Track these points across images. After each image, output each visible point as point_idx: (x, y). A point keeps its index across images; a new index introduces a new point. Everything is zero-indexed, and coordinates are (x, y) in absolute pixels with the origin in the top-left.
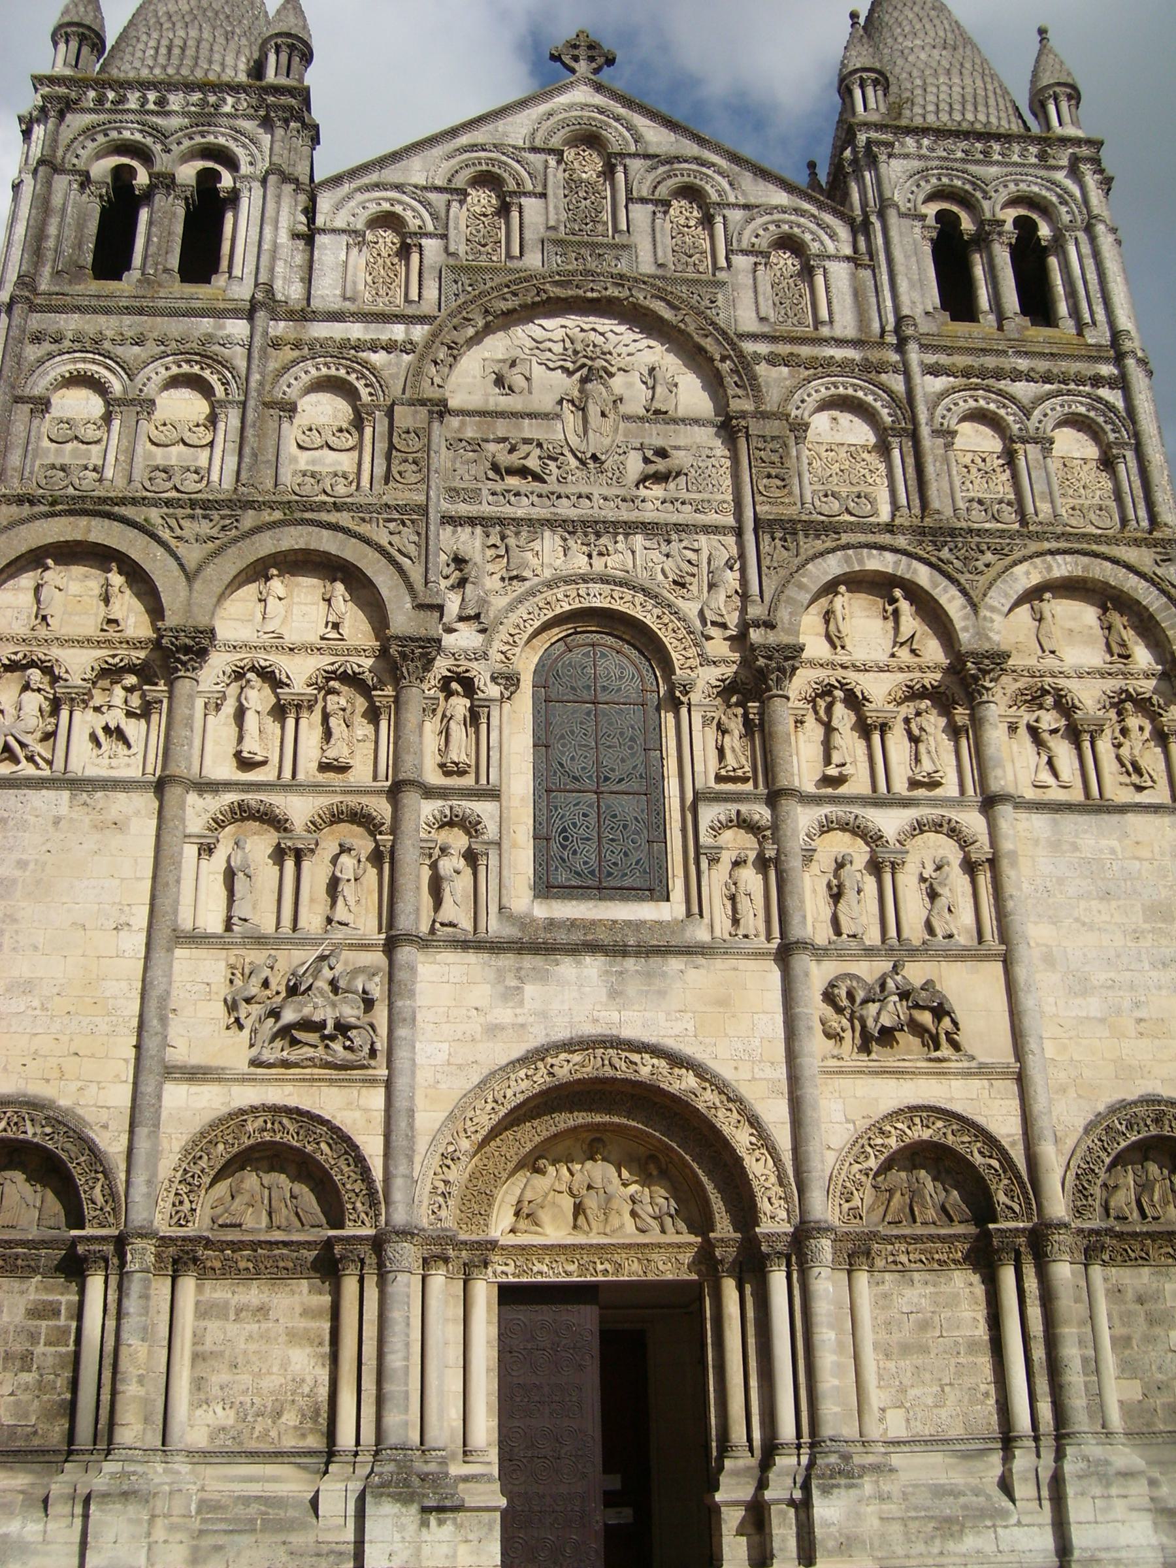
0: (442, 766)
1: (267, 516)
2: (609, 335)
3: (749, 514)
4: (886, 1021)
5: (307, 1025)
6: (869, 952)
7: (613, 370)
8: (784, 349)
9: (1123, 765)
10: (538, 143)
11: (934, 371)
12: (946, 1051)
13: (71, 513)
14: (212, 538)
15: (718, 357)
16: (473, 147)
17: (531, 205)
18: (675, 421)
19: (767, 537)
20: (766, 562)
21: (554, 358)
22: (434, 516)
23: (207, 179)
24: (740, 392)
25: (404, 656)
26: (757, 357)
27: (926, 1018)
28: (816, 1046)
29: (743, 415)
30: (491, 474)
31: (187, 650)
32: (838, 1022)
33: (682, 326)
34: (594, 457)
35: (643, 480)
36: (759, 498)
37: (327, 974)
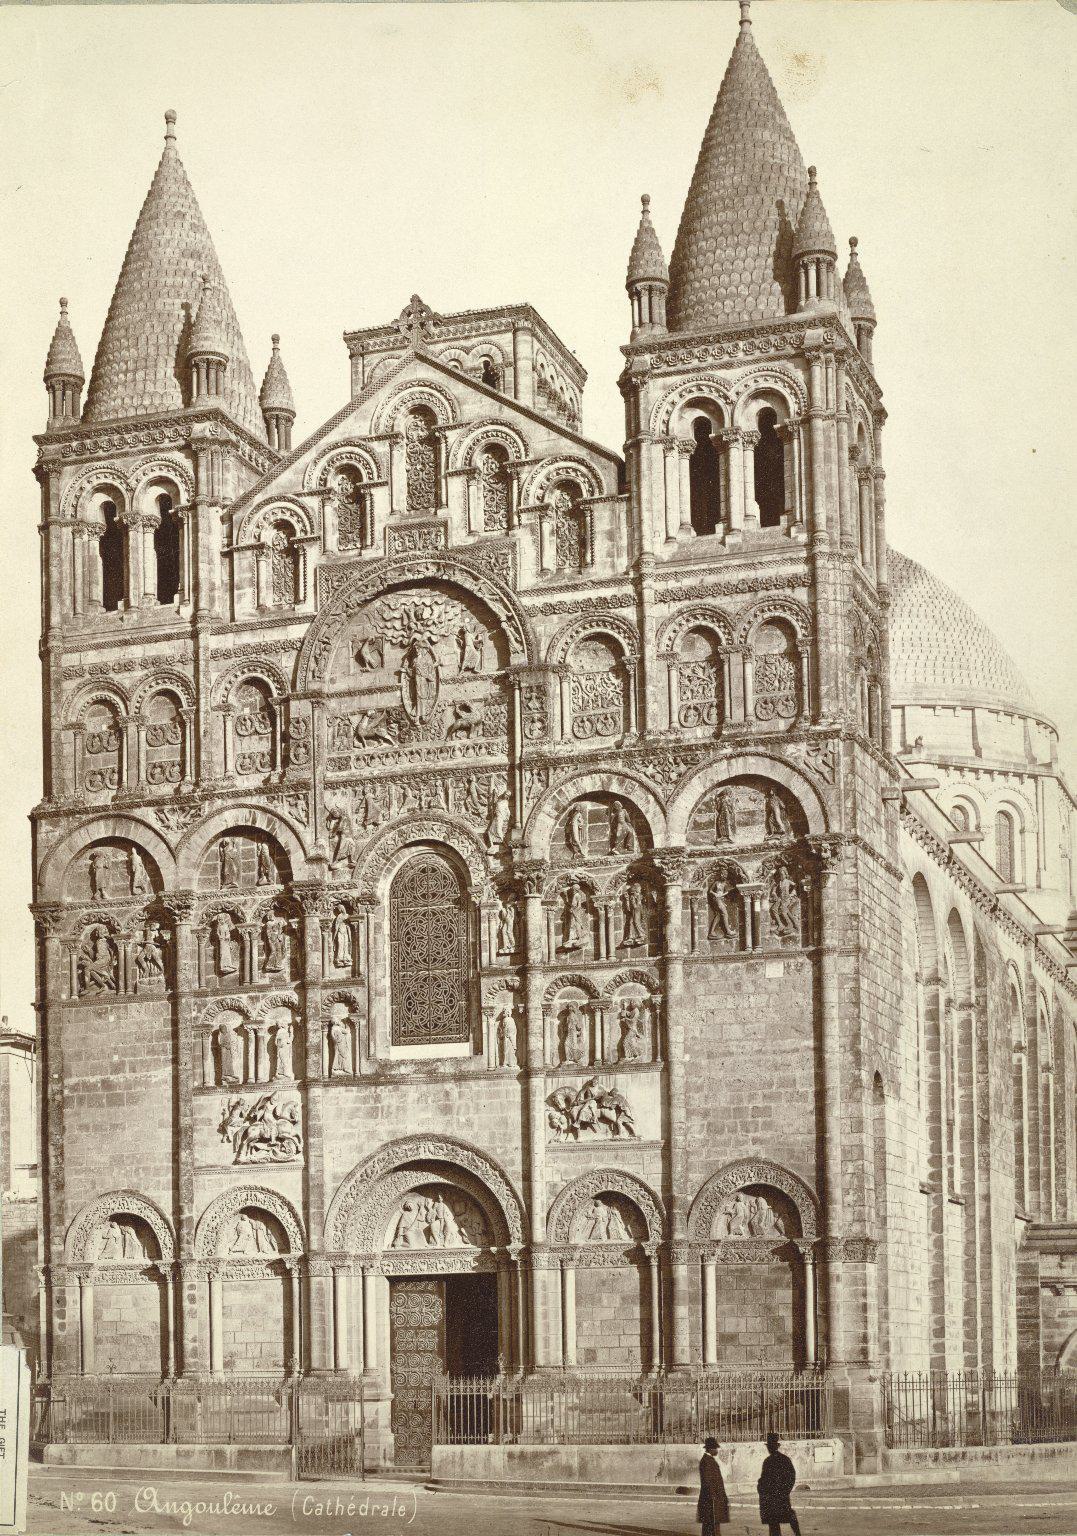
0: (335, 963)
1: (219, 803)
2: (435, 607)
3: (518, 754)
4: (583, 1118)
5: (262, 1139)
6: (580, 1071)
7: (434, 639)
8: (555, 598)
9: (773, 917)
10: (382, 430)
11: (663, 598)
12: (624, 1133)
13: (101, 818)
14: (185, 825)
15: (504, 618)
16: (336, 446)
17: (380, 495)
18: (475, 679)
19: (528, 775)
20: (525, 794)
21: (396, 634)
22: (320, 786)
23: (165, 502)
24: (517, 646)
25: (302, 898)
26: (531, 612)
27: (612, 1115)
28: (541, 1135)
29: (518, 671)
30: (357, 743)
31: (179, 907)
32: (561, 1119)
33: (479, 595)
34: (422, 722)
35: (452, 731)
36: (525, 741)
37: (270, 1108)
